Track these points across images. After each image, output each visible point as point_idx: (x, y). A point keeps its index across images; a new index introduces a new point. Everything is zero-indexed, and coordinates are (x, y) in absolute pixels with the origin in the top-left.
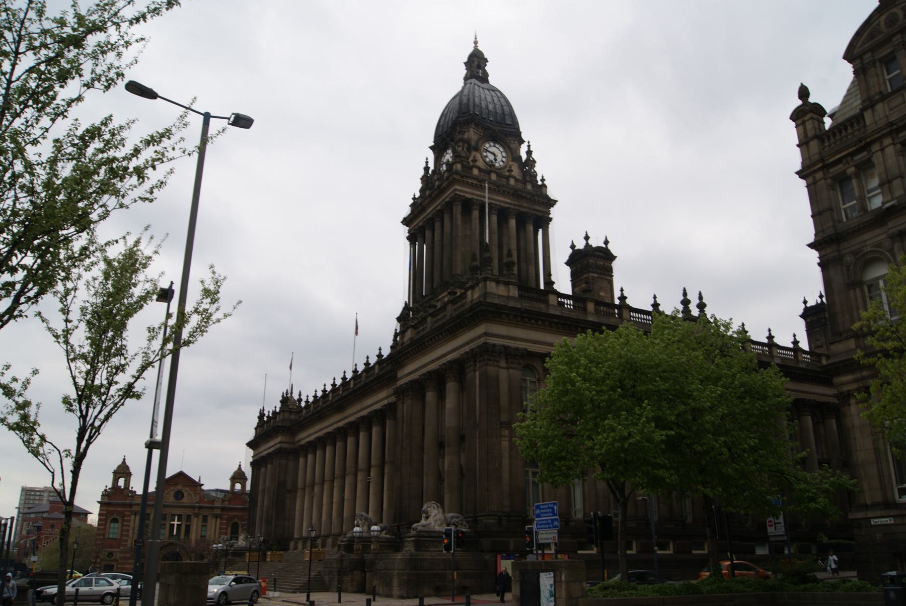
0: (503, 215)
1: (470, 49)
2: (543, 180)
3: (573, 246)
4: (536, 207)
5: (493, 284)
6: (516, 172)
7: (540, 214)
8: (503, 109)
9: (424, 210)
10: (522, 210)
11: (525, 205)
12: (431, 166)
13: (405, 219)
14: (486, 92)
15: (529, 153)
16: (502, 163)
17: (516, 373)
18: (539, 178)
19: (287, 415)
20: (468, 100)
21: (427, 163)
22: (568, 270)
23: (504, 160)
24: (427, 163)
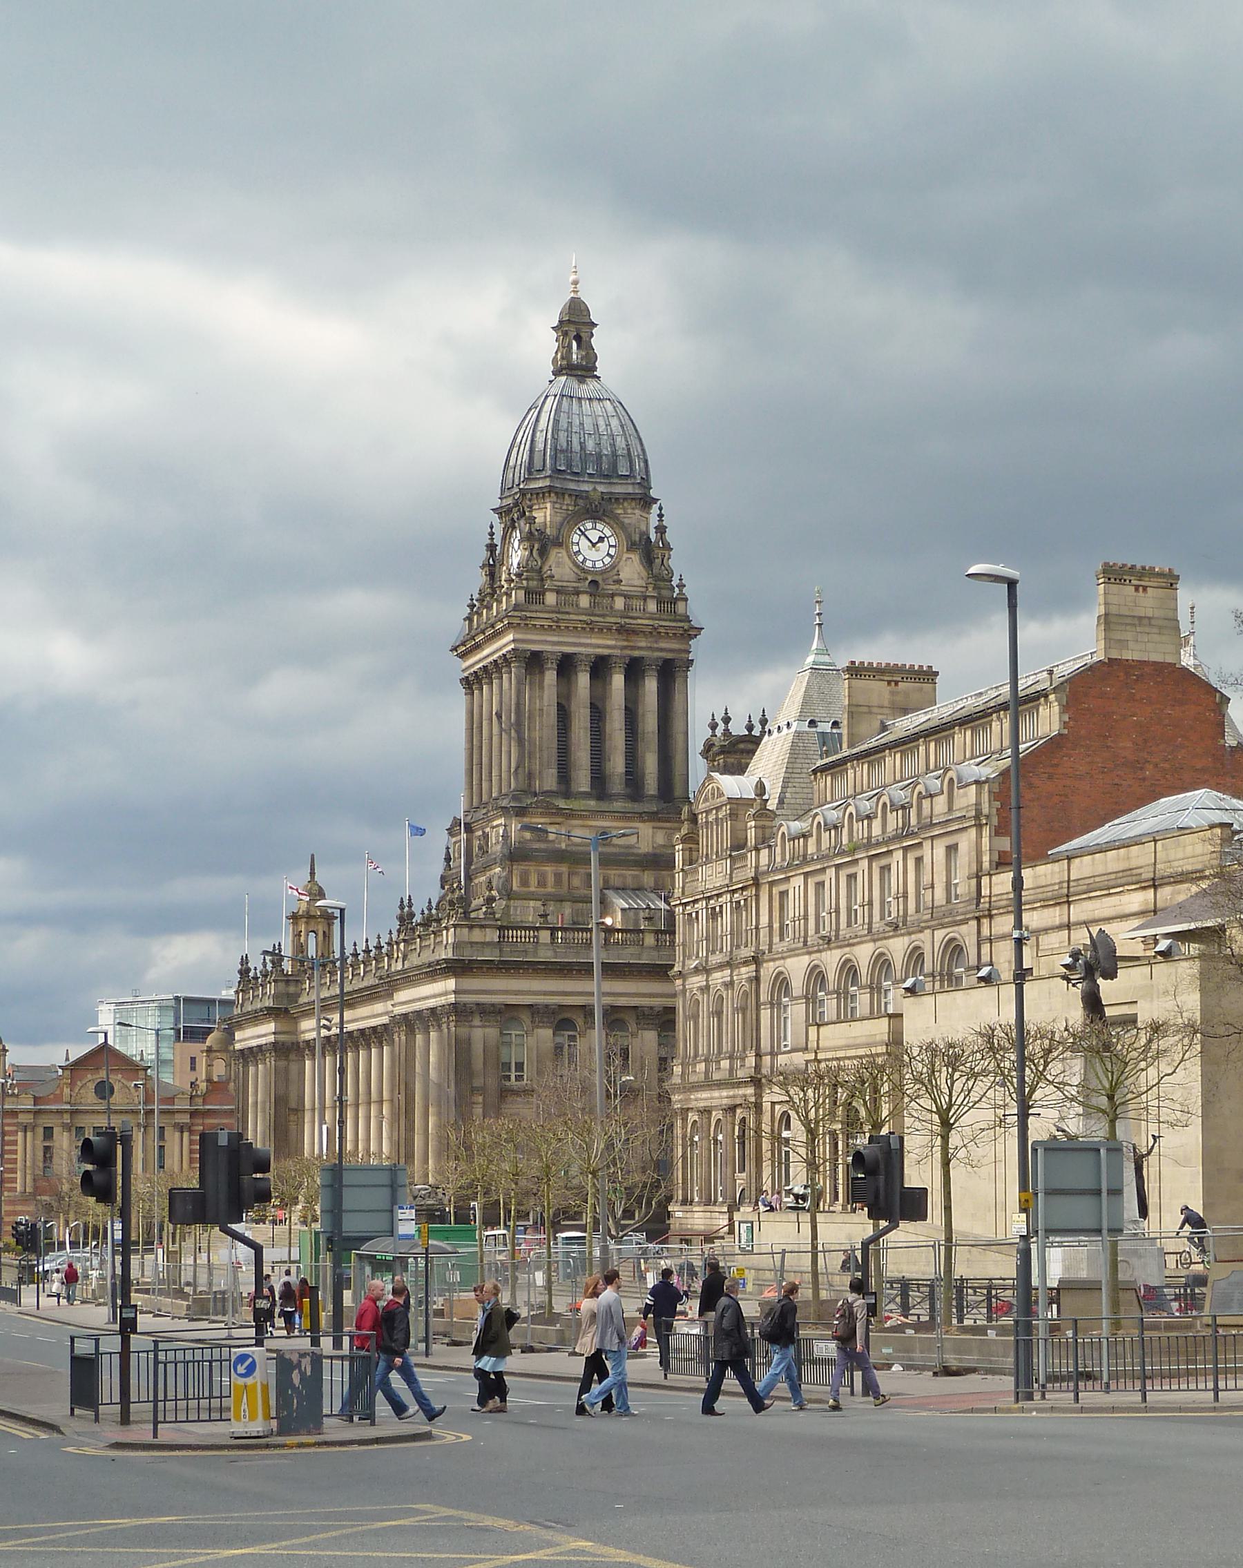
0: (600, 668)
2: (681, 586)
3: (714, 726)
4: (663, 645)
5: (466, 930)
6: (632, 571)
7: (669, 656)
8: (613, 445)
9: (478, 647)
10: (636, 653)
11: (643, 644)
12: (497, 540)
14: (586, 404)
15: (661, 530)
16: (607, 560)
17: (492, 1032)
18: (675, 582)
19: (281, 986)
21: (492, 534)
23: (612, 551)
24: (492, 534)
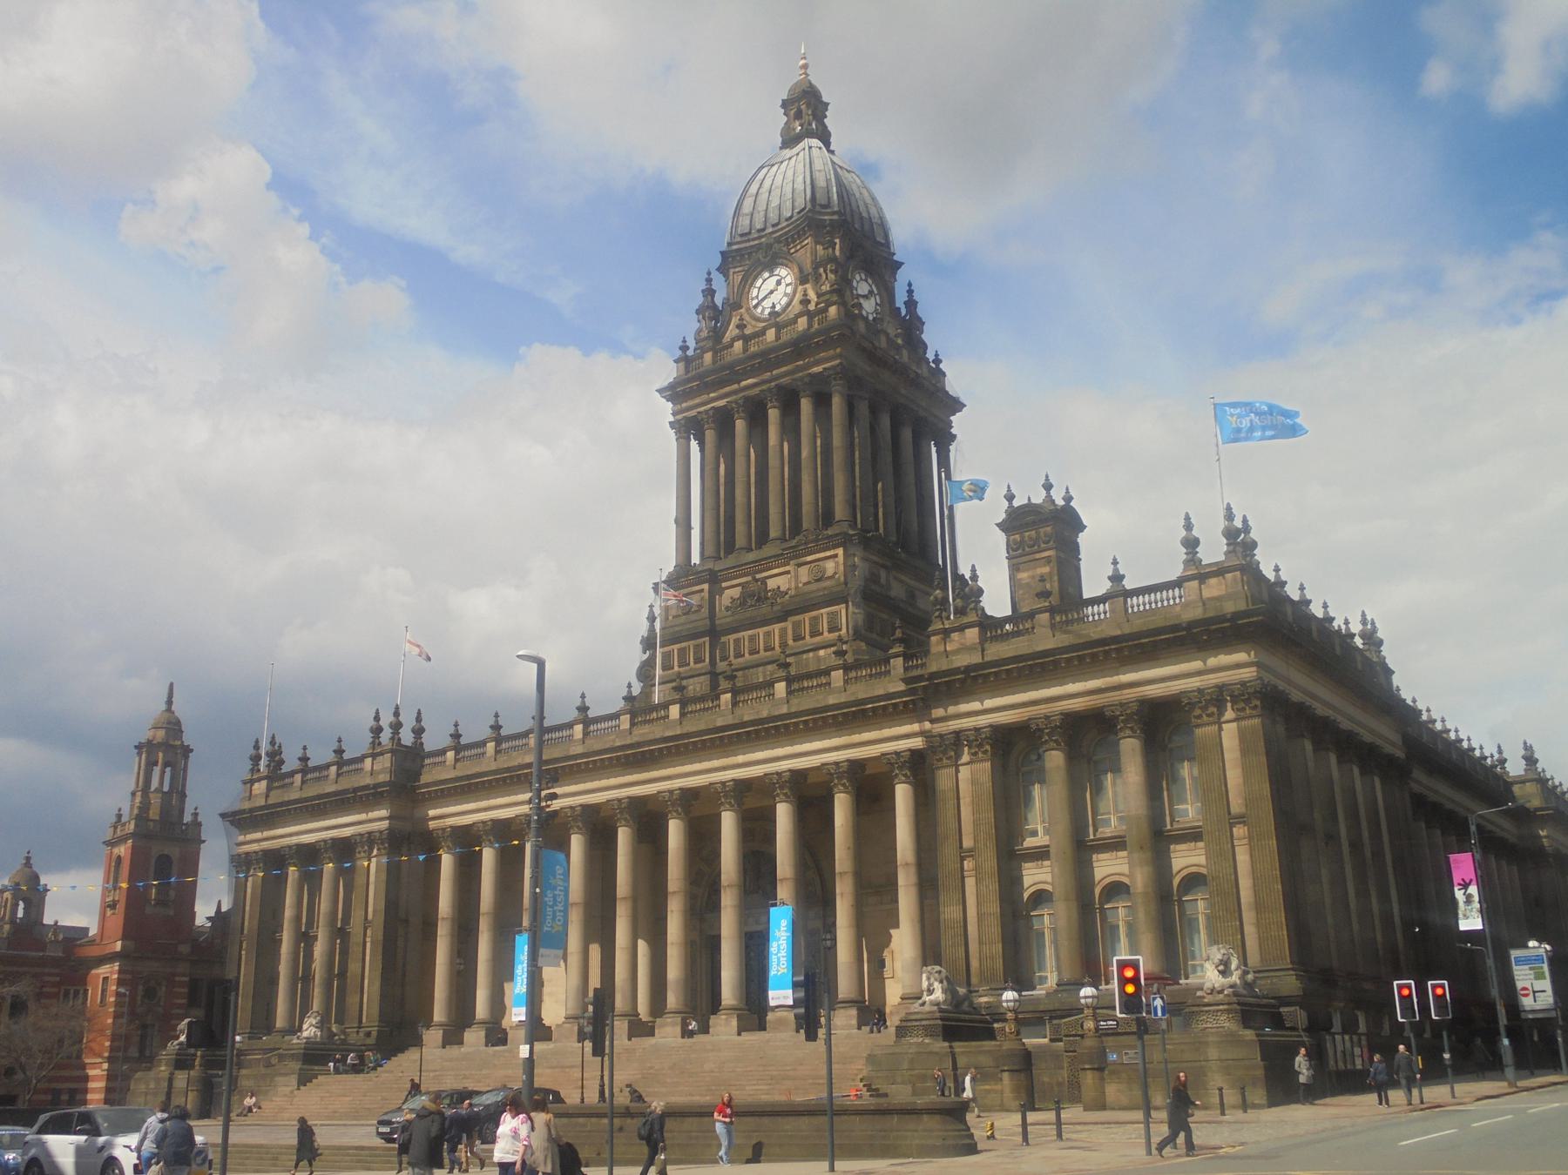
1: (797, 77)
2: (937, 361)
3: (1010, 497)
13: (671, 387)
15: (911, 304)
18: (930, 356)
20: (828, 181)
21: (709, 281)
22: (1000, 538)
24: (709, 281)
